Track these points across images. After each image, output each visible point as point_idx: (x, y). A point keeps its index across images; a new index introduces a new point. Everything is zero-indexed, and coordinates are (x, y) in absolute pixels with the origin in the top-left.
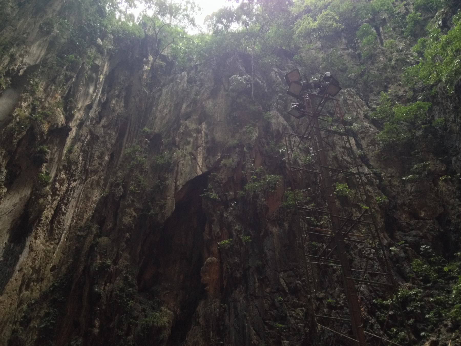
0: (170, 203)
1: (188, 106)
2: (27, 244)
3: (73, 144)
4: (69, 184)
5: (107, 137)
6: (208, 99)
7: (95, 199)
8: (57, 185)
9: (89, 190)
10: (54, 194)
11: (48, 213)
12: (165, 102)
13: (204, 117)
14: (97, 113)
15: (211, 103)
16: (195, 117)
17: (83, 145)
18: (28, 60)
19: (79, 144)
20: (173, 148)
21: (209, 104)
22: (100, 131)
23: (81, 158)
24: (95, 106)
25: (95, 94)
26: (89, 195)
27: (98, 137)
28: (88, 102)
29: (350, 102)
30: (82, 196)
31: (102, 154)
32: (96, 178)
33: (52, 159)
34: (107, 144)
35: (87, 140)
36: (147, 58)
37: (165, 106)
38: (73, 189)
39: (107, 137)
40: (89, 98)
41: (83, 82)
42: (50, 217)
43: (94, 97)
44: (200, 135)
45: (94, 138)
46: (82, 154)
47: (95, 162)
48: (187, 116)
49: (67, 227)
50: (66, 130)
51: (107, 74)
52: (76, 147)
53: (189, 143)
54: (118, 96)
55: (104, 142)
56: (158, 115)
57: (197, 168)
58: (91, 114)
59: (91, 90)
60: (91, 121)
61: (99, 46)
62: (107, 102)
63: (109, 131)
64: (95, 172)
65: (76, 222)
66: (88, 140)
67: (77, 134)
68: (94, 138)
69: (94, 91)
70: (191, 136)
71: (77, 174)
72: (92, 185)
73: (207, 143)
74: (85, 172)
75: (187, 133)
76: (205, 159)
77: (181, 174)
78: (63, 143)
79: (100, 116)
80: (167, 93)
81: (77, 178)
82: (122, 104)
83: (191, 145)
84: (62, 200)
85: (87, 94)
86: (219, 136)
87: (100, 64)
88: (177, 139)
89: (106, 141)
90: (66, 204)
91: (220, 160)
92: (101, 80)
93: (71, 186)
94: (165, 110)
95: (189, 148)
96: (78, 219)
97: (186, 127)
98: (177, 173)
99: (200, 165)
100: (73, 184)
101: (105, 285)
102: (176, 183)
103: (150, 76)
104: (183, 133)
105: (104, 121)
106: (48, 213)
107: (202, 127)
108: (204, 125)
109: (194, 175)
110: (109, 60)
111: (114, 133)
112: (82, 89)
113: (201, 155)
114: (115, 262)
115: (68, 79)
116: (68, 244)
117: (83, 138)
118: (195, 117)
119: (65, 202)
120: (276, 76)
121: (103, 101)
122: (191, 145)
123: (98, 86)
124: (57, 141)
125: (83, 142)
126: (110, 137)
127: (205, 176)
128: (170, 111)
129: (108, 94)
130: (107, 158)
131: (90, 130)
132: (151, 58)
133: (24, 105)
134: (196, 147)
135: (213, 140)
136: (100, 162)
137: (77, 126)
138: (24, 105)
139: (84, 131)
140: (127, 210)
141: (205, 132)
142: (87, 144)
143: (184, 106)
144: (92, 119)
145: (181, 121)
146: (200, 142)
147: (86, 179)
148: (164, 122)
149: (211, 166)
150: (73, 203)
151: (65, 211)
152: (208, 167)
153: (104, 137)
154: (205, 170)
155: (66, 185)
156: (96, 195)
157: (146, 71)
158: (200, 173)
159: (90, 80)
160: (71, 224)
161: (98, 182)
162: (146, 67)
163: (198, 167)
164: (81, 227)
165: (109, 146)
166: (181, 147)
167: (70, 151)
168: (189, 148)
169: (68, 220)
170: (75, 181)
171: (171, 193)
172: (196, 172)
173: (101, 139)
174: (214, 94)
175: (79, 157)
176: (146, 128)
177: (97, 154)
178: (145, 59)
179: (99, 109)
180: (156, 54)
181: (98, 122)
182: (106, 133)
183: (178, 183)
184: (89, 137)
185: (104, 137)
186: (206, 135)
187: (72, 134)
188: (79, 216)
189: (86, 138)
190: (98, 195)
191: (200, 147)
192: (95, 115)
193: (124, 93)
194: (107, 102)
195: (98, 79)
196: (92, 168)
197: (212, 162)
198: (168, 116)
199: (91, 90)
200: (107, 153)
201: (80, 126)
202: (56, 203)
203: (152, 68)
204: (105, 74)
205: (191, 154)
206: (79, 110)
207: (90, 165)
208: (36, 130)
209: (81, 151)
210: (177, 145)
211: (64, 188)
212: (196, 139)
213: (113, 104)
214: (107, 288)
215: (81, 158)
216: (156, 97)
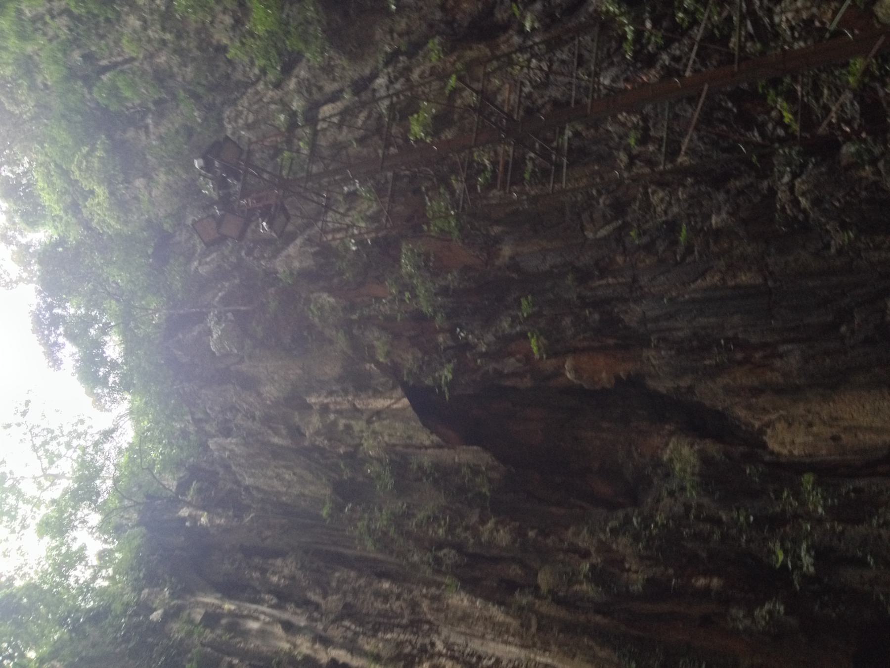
0: (466, 455)
1: (276, 433)
3: (364, 654)
4: (440, 655)
5: (345, 587)
6: (259, 394)
7: (466, 603)
9: (450, 615)
12: (271, 478)
13: (295, 401)
14: (299, 611)
15: (267, 388)
17: (364, 634)
20: (360, 456)
21: (271, 391)
22: (333, 602)
23: (389, 636)
24: (285, 616)
25: (262, 617)
26: (460, 614)
27: (346, 606)
28: (278, 630)
29: (251, 118)
30: (462, 628)
31: (377, 594)
32: (425, 605)
34: (360, 586)
35: (353, 627)
36: (184, 520)
37: (278, 477)
38: (449, 646)
39: (345, 587)
40: (269, 628)
41: (240, 642)
43: (268, 619)
44: (332, 406)
45: (348, 612)
46: (380, 635)
47: (394, 607)
48: (296, 433)
51: (219, 595)
52: (367, 648)
53: (348, 427)
54: (264, 571)
55: (355, 592)
56: (296, 490)
57: (397, 409)
58: (302, 621)
59: (254, 625)
60: (316, 620)
61: (166, 617)
63: (334, 584)
64: (414, 606)
65: (513, 636)
66: (354, 623)
67: (342, 647)
68: (348, 612)
69: (257, 619)
70: (334, 423)
71: (420, 641)
72: (438, 610)
73: (346, 392)
74: (415, 625)
75: (330, 431)
77: (410, 437)
79: (305, 604)
80: (253, 475)
81: (427, 641)
82: (279, 562)
83: (353, 422)
85: (262, 633)
86: (332, 370)
87: (202, 611)
88: (341, 451)
89: (354, 589)
90: (480, 658)
91: (378, 364)
92: (233, 607)
93: (444, 651)
94: (287, 477)
95: (358, 425)
96: (507, 632)
97: (317, 433)
98: (407, 446)
99: (387, 402)
100: (440, 646)
101: (629, 570)
102: (426, 448)
103: (220, 510)
104: (330, 440)
105: (314, 596)
107: (315, 404)
108: (312, 400)
109: (411, 412)
110: (193, 594)
111: (337, 574)
112: (253, 644)
113: (371, 401)
114: (585, 555)
116: (554, 648)
118: (297, 418)
119: (474, 660)
120: (207, 263)
121: (275, 601)
122: (353, 422)
123: (245, 613)
125: (356, 634)
126: (345, 581)
127: (411, 392)
128: (287, 467)
129: (259, 592)
130: (386, 585)
131: (333, 622)
132: (184, 512)
134: (355, 412)
135: (340, 380)
136: (394, 598)
137: (327, 648)
139: (335, 633)
140: (485, 538)
141: (326, 397)
142: (361, 624)
143: (276, 440)
144: (311, 619)
145: (306, 443)
146: (346, 406)
147: (429, 622)
148: (309, 477)
149: (391, 382)
150: (476, 645)
151: (493, 660)
152: (394, 388)
153: (345, 594)
154: (399, 392)
156: (460, 600)
157: (210, 520)
158: (405, 401)
159: (235, 626)
160: (516, 645)
161: (434, 599)
162: (204, 520)
163: (395, 406)
164: (522, 625)
165: (362, 582)
166: (357, 441)
168: (358, 425)
169: (510, 652)
170: (433, 644)
171: (449, 456)
172: (404, 409)
173: (350, 599)
174: (249, 383)
175: (387, 640)
176: (324, 513)
177: (379, 605)
178: (188, 524)
179: (291, 607)
180: (175, 501)
181: (317, 607)
182: (337, 590)
183: (427, 443)
184: (347, 623)
185: (345, 594)
186: (331, 393)
188: (500, 632)
189: (348, 628)
190: (458, 598)
191: (354, 405)
192: (302, 613)
193: (257, 560)
195: (231, 613)
196: (407, 613)
197: (382, 380)
198: (298, 471)
199: (254, 625)
200: (376, 585)
201: (326, 642)
203: (204, 508)
204: (221, 599)
205: (369, 422)
206: (295, 646)
207: (402, 616)
209: (374, 636)
210: (352, 450)
212: (340, 412)
213: (279, 580)
214: (634, 568)
215: (389, 636)
216: (260, 496)
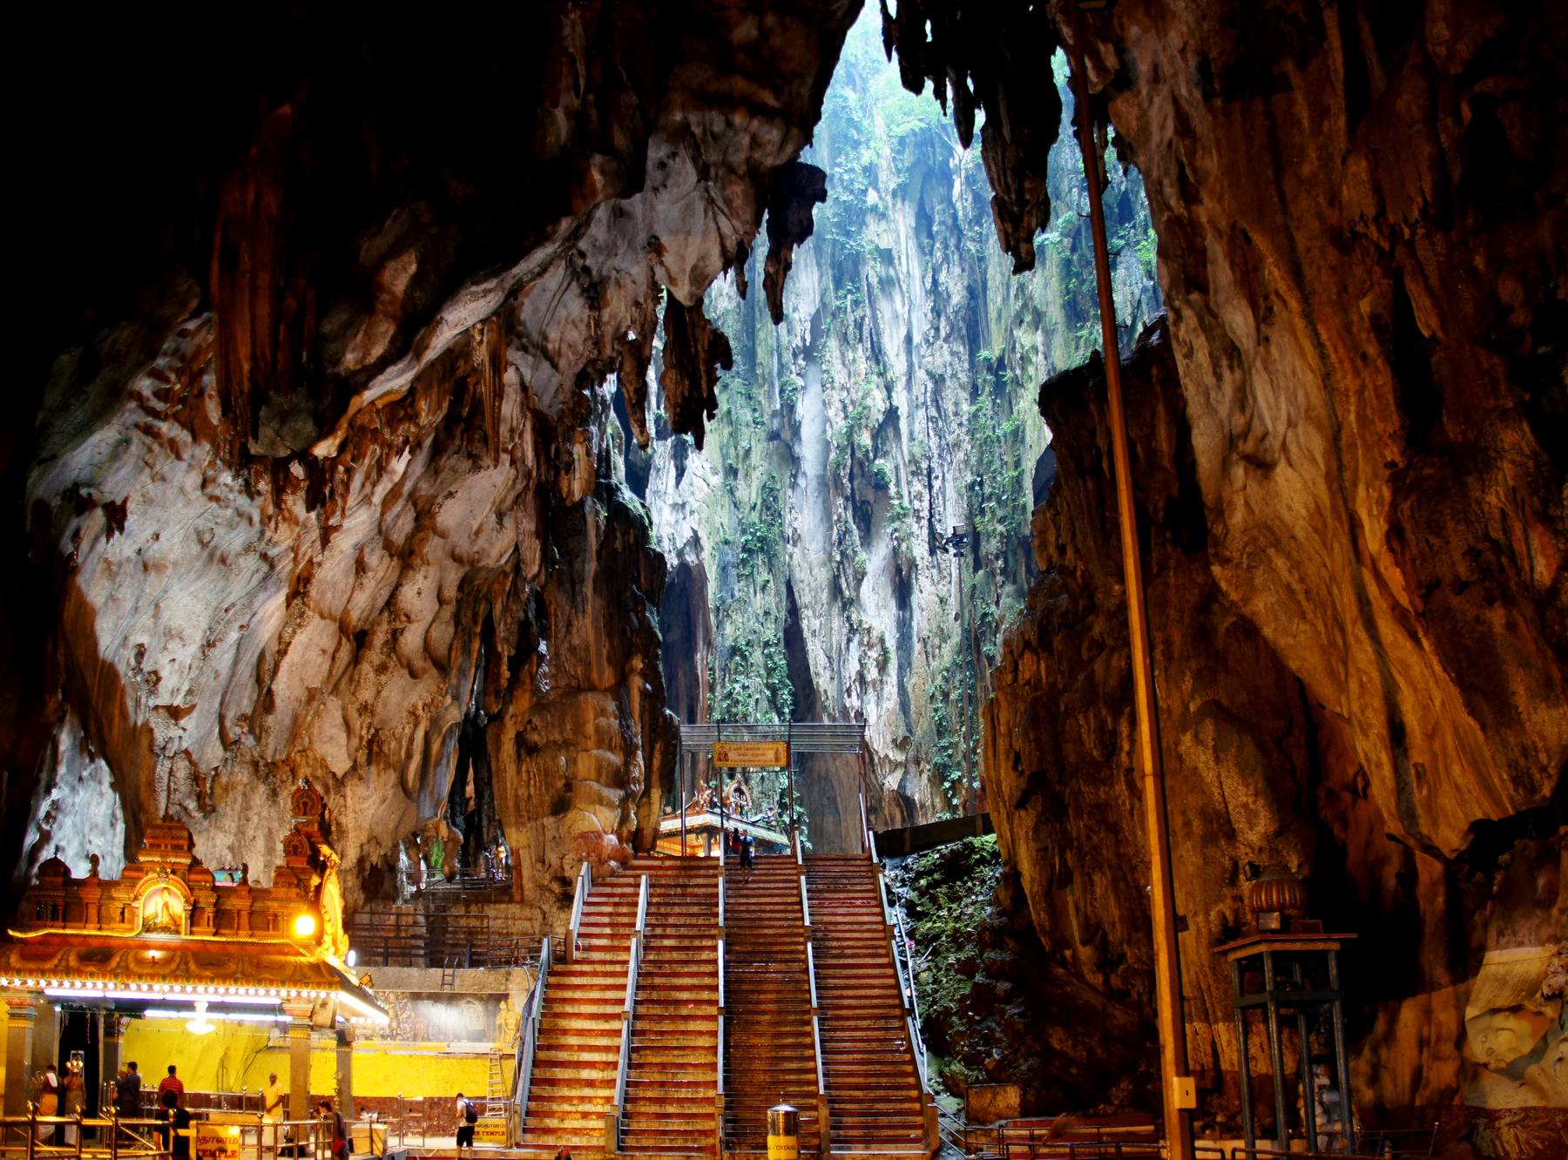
2: (914, 606)
8: (917, 504)
10: (919, 519)
19: (921, 413)
31: (956, 404)
42: (926, 554)
55: (954, 375)
62: (935, 282)
64: (957, 445)
67: (910, 402)
68: (938, 381)
84: (930, 521)
117: (921, 400)
121: (928, 286)
125: (924, 403)
155: (927, 497)
167: (912, 438)
184: (930, 386)
193: (952, 242)
194: (935, 282)
200: (964, 395)
202: (925, 531)
211: (926, 504)
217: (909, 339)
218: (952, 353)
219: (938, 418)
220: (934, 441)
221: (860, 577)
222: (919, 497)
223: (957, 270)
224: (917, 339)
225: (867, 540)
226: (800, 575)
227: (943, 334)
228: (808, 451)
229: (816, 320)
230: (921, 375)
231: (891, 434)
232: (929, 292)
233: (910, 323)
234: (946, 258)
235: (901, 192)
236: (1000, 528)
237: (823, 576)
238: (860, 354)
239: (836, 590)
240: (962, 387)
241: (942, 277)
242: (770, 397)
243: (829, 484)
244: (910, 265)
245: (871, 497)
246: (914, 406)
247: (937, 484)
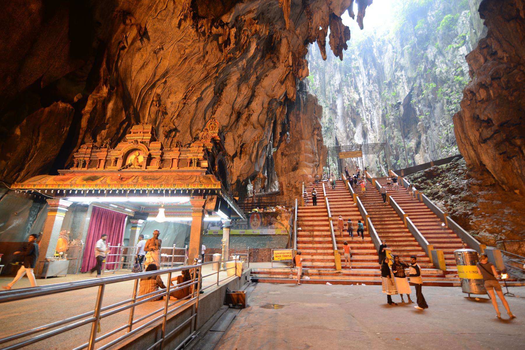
10: (368, 120)
11: (369, 127)
16: (399, 69)
18: (338, 82)
19: (367, 99)
31: (376, 96)
33: (362, 110)
38: (373, 114)
45: (371, 92)
49: (377, 126)
50: (360, 99)
55: (375, 90)
62: (368, 73)
64: (377, 104)
68: (371, 92)
74: (374, 105)
76: (408, 86)
78: (362, 103)
79: (369, 79)
85: (360, 80)
86: (409, 75)
106: (369, 127)
115: (352, 82)
124: (360, 103)
130: (378, 96)
133: (345, 101)
138: (345, 101)
156: (381, 112)
159: (358, 73)
165: (377, 91)
168: (401, 84)
177: (374, 97)
187: (363, 99)
193: (372, 64)
194: (368, 73)
201: (364, 93)
208: (353, 108)
211: (370, 117)
217: (363, 84)
218: (374, 86)
219: (371, 100)
220: (370, 105)
221: (354, 133)
222: (368, 115)
223: (374, 69)
224: (365, 84)
225: (355, 126)
226: (339, 136)
227: (371, 83)
228: (339, 111)
229: (340, 85)
230: (366, 91)
231: (360, 103)
232: (366, 75)
233: (363, 81)
234: (371, 68)
235: (360, 55)
236: (393, 117)
237: (344, 135)
238: (352, 89)
239: (348, 137)
240: (377, 92)
241: (370, 71)
242: (329, 101)
243: (345, 116)
244: (362, 69)
245: (356, 117)
246: (365, 98)
247: (372, 113)
